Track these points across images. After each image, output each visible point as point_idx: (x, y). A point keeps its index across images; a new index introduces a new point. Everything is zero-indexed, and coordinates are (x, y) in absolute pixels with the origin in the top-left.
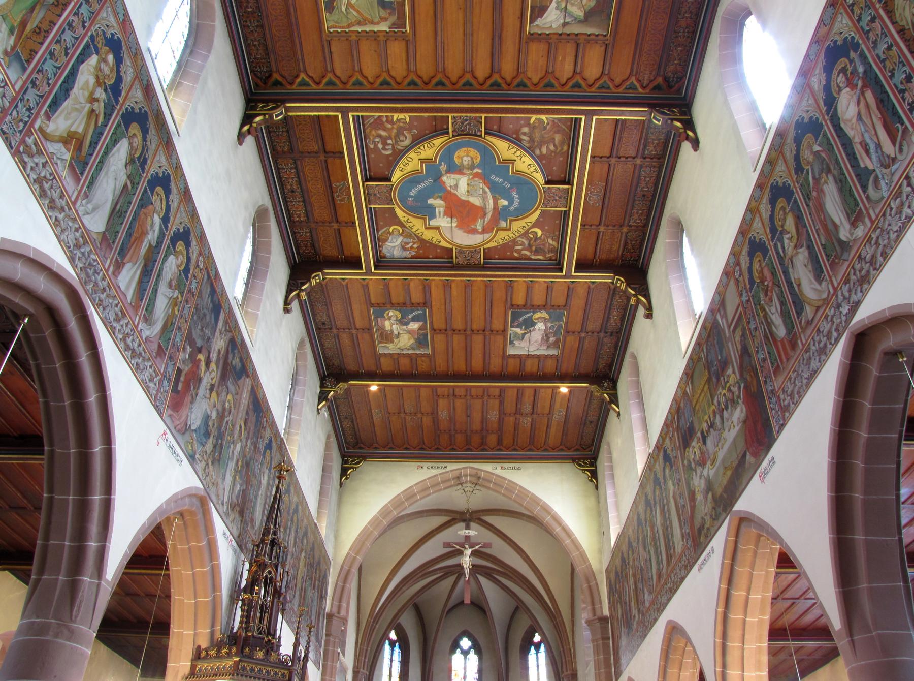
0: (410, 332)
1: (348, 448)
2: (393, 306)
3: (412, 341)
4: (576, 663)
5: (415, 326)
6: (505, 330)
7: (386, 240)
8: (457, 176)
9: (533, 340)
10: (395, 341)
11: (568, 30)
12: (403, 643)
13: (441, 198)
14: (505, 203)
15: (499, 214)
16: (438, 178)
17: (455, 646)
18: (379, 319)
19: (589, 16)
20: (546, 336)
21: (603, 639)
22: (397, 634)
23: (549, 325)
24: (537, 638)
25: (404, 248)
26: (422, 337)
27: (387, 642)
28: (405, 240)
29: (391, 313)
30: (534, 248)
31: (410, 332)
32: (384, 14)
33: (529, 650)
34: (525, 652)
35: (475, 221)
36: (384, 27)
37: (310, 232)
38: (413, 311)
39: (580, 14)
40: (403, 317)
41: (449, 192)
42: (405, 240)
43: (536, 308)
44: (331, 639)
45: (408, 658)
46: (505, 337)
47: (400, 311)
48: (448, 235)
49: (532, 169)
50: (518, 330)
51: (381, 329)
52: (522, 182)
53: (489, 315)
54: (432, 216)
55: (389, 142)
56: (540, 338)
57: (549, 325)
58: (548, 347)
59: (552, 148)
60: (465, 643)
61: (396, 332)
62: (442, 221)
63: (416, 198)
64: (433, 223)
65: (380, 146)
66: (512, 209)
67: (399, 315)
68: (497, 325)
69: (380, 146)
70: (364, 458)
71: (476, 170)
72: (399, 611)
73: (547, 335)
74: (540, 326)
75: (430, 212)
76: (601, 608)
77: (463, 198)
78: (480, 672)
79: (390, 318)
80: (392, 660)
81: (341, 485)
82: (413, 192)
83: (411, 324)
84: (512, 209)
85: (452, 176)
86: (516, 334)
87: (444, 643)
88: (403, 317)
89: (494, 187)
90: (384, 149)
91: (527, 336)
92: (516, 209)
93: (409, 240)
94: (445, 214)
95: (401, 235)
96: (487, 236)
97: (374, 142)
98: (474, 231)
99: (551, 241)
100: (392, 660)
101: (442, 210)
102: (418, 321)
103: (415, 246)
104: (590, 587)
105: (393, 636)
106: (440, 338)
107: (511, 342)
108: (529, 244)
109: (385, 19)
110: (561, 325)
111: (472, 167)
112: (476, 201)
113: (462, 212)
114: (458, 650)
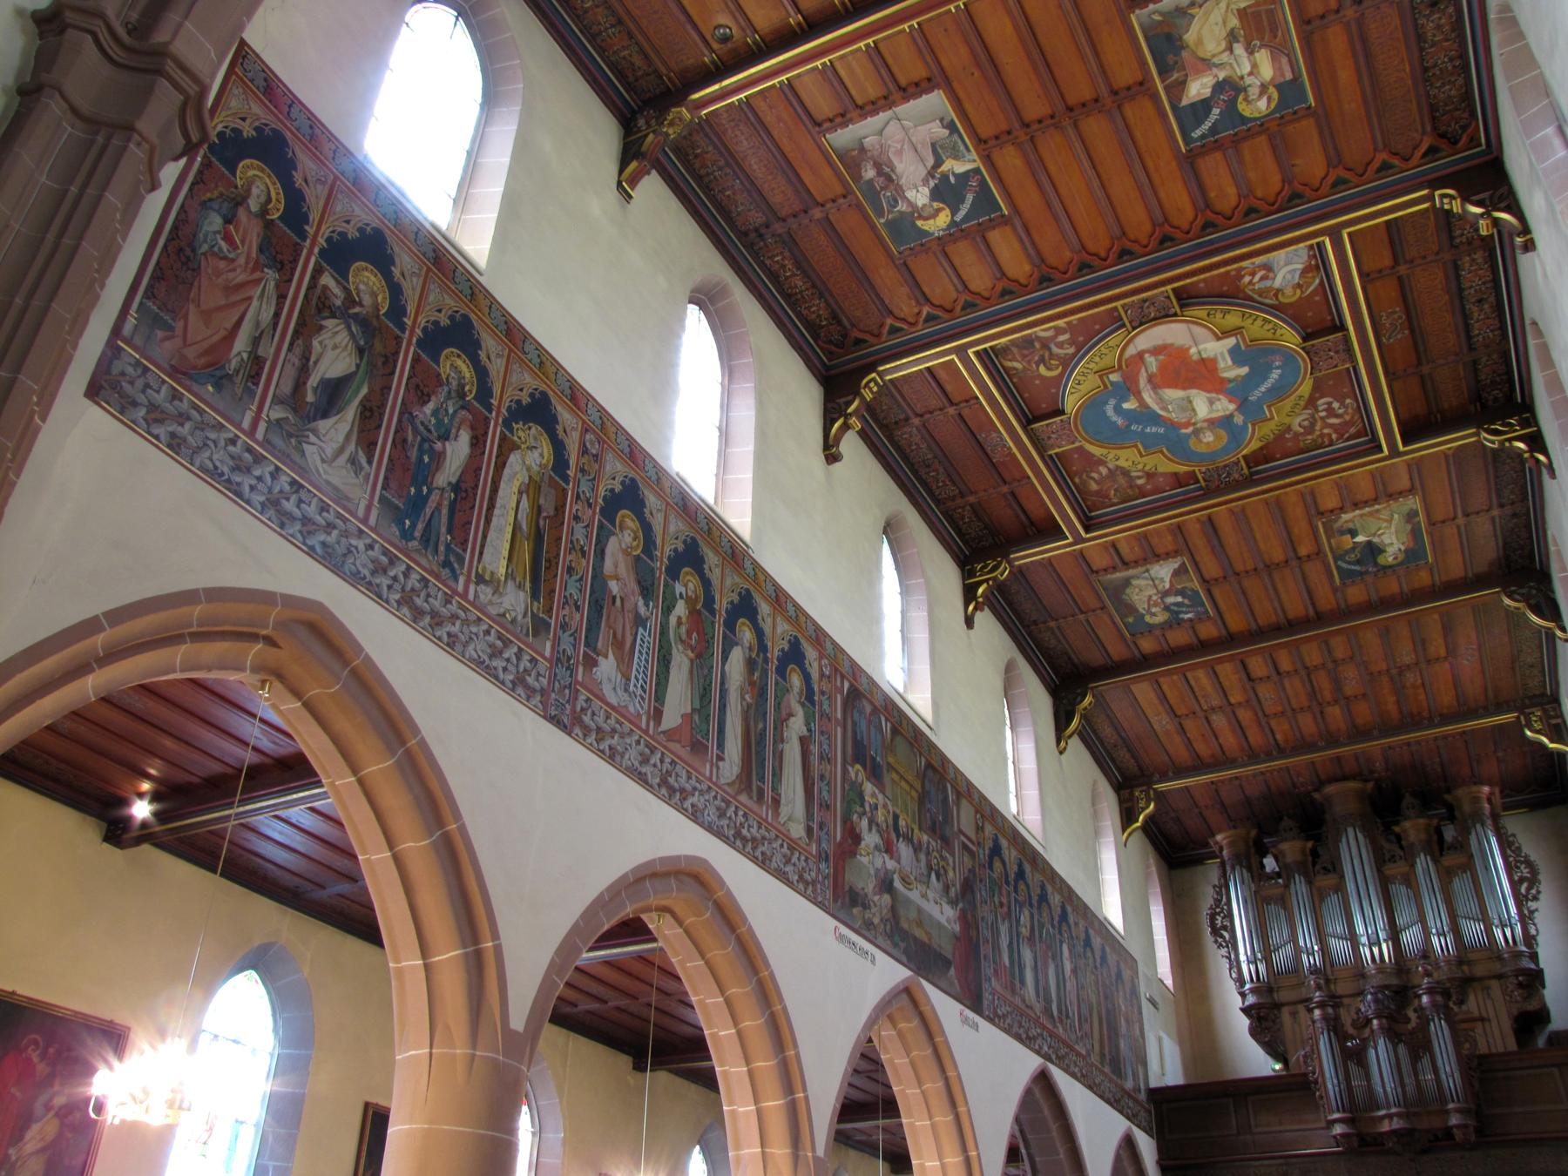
0: (1206, 64)
2: (1262, 126)
3: (1190, 37)
5: (1198, 88)
6: (988, 159)
7: (1304, 272)
8: (1214, 415)
9: (908, 155)
10: (1234, 22)
11: (1141, 569)
13: (1230, 381)
14: (1126, 406)
15: (1129, 387)
16: (1243, 405)
18: (1289, 76)
19: (1127, 583)
20: (888, 176)
23: (902, 207)
25: (1268, 268)
26: (1171, 59)
28: (1268, 283)
29: (1262, 105)
30: (1037, 345)
31: (1206, 64)
32: (1351, 525)
35: (1162, 367)
36: (1345, 517)
37: (1452, 238)
38: (1214, 130)
39: (1134, 582)
40: (1231, 109)
41: (1218, 391)
42: (1268, 283)
43: (956, 233)
46: (980, 142)
47: (1244, 120)
48: (1197, 330)
49: (1111, 456)
50: (961, 168)
51: (1279, 49)
52: (1117, 438)
53: (1037, 167)
54: (1234, 352)
55: (1323, 414)
56: (900, 167)
57: (902, 207)
58: (862, 149)
59: (1095, 475)
61: (1239, 49)
62: (1216, 349)
63: (1269, 368)
64: (1231, 341)
65: (1336, 405)
66: (1112, 402)
67: (1244, 109)
68: (1010, 159)
69: (1336, 405)
71: (1190, 429)
73: (889, 179)
74: (920, 196)
75: (1237, 355)
77: (1193, 392)
79: (1264, 88)
82: (1275, 375)
83: (1207, 92)
84: (1112, 402)
85: (1221, 414)
86: (956, 158)
88: (1233, 101)
89: (1155, 419)
90: (1330, 404)
91: (931, 161)
92: (1106, 403)
93: (1262, 285)
94: (1214, 361)
95: (1278, 291)
96: (1131, 351)
97: (1346, 407)
98: (1156, 351)
99: (1016, 364)
101: (1222, 365)
102: (1193, 105)
103: (1247, 279)
106: (1125, 76)
107: (951, 126)
108: (1050, 349)
109: (1351, 521)
110: (880, 214)
111: (1197, 432)
112: (1172, 394)
113: (1187, 371)
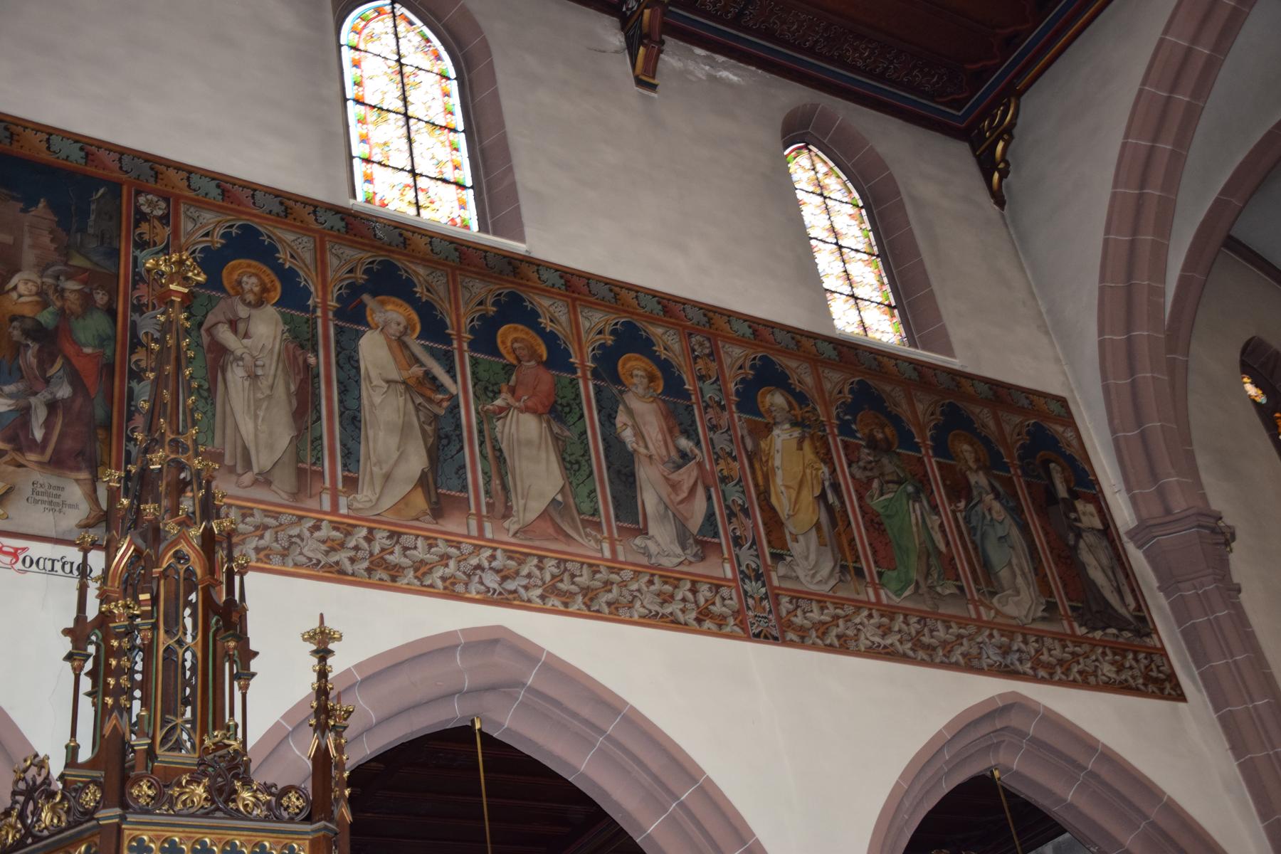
1: (958, 105)
70: (1013, 92)
81: (999, 199)
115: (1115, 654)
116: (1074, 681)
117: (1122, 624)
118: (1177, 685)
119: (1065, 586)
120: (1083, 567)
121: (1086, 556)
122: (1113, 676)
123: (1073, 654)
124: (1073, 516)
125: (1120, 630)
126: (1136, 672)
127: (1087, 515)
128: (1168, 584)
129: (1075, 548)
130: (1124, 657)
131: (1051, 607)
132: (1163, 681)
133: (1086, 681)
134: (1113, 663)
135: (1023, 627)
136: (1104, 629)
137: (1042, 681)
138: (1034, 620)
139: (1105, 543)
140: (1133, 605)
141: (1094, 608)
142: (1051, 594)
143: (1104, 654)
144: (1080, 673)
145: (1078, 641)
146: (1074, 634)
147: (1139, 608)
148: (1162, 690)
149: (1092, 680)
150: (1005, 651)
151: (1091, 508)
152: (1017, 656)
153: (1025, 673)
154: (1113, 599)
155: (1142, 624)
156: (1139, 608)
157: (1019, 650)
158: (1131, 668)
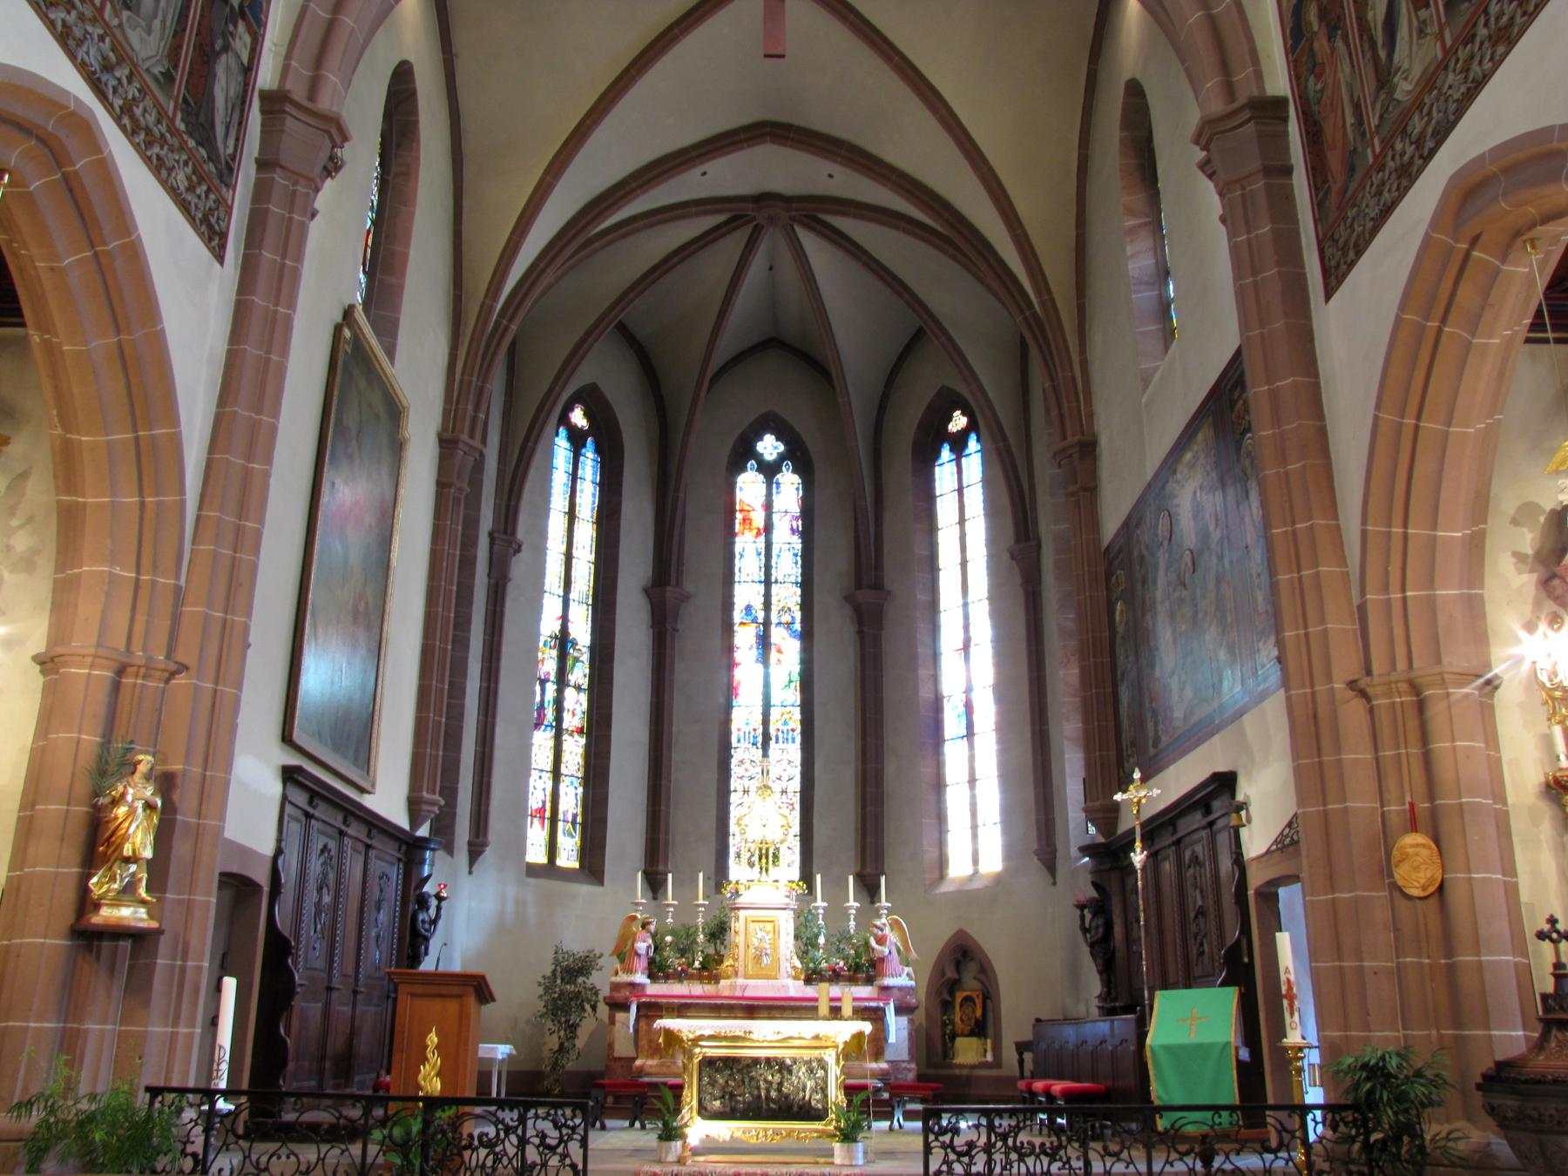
4: (1091, 415)
12: (605, 438)
17: (743, 454)
21: (1268, 171)
22: (586, 415)
24: (958, 422)
27: (563, 432)
33: (937, 455)
34: (925, 460)
44: (279, 178)
45: (621, 467)
60: (769, 447)
72: (588, 334)
76: (1259, 76)
78: (808, 511)
80: (574, 477)
87: (712, 442)
100: (574, 477)
104: (1213, 23)
105: (578, 418)
114: (752, 463)
115: (194, 172)
116: (149, 158)
117: (213, 157)
118: (223, 247)
119: (190, 73)
120: (210, 77)
121: (220, 69)
122: (182, 188)
123: (162, 135)
124: (231, 28)
125: (210, 158)
126: (201, 205)
127: (242, 42)
128: (263, 164)
129: (218, 55)
130: (199, 183)
131: (168, 78)
132: (216, 233)
133: (158, 167)
134: (188, 178)
135: (135, 66)
136: (198, 143)
137: (123, 128)
138: (147, 70)
139: (241, 79)
140: (230, 150)
141: (202, 119)
142: (176, 67)
143: (186, 163)
144: (159, 158)
145: (173, 130)
146: (172, 120)
147: (233, 157)
148: (211, 239)
149: (164, 173)
150: (108, 68)
151: (248, 39)
152: (114, 82)
153: (112, 105)
154: (220, 130)
155: (227, 172)
156: (233, 157)
157: (119, 80)
158: (199, 197)
